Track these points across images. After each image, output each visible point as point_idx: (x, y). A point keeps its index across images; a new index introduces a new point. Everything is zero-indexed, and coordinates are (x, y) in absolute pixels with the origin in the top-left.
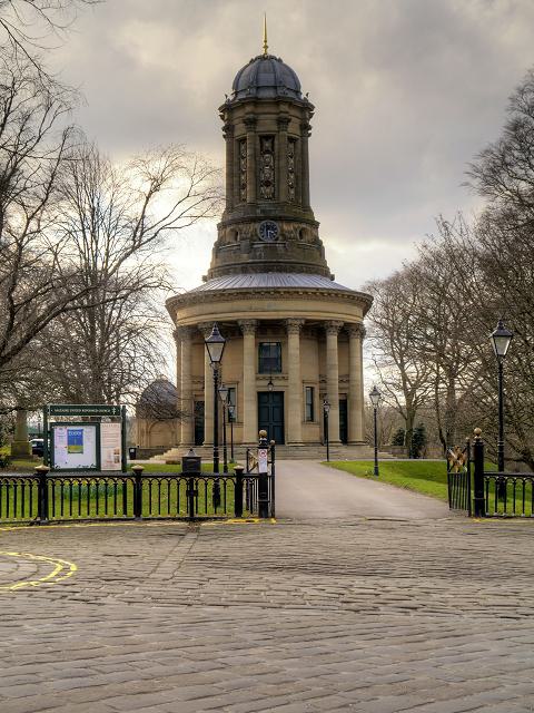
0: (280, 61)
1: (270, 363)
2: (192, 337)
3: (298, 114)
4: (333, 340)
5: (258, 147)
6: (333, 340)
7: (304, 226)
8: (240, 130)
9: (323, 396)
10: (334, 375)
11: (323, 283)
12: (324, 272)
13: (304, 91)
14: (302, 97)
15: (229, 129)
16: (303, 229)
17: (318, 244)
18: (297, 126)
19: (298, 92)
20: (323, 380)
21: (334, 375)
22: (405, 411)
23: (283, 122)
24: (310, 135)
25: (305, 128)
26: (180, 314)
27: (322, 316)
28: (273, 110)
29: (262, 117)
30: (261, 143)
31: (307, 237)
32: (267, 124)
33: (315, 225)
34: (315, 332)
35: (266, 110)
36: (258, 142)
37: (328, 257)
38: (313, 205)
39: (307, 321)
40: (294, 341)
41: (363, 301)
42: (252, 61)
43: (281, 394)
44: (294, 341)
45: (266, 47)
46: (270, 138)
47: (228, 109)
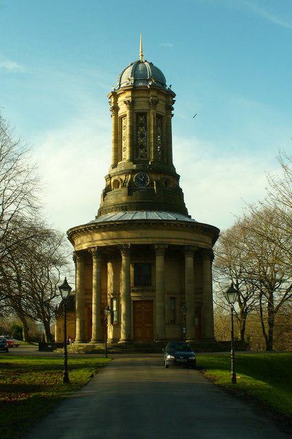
0: (151, 64)
1: (142, 279)
2: (83, 257)
3: (163, 98)
4: (189, 261)
5: (135, 121)
6: (189, 261)
7: (167, 177)
8: (124, 109)
9: (182, 304)
10: (189, 287)
11: (182, 218)
12: (184, 211)
13: (168, 84)
14: (167, 88)
15: (115, 109)
16: (167, 179)
17: (179, 193)
18: (163, 107)
19: (164, 85)
20: (183, 292)
21: (189, 287)
22: (239, 316)
23: (155, 103)
24: (173, 115)
25: (169, 108)
26: (78, 241)
27: (181, 243)
28: (145, 94)
29: (139, 100)
30: (137, 119)
31: (171, 186)
32: (142, 106)
33: (178, 177)
34: (175, 254)
35: (141, 95)
36: (135, 116)
37: (186, 200)
38: (175, 163)
39: (171, 247)
40: (159, 261)
41: (212, 232)
42: (132, 64)
43: (152, 301)
44: (159, 261)
45: (142, 56)
46: (143, 114)
47: (115, 95)
